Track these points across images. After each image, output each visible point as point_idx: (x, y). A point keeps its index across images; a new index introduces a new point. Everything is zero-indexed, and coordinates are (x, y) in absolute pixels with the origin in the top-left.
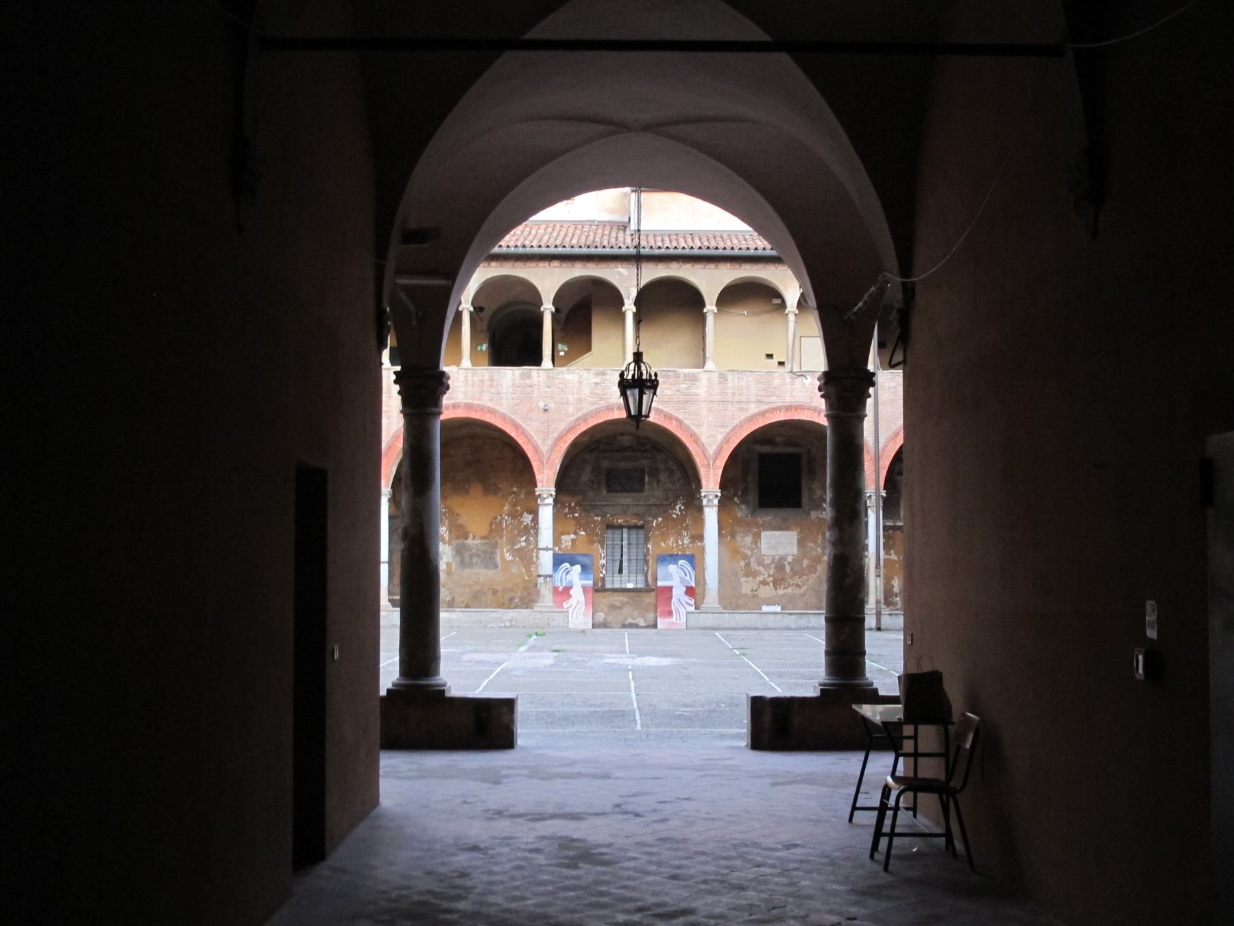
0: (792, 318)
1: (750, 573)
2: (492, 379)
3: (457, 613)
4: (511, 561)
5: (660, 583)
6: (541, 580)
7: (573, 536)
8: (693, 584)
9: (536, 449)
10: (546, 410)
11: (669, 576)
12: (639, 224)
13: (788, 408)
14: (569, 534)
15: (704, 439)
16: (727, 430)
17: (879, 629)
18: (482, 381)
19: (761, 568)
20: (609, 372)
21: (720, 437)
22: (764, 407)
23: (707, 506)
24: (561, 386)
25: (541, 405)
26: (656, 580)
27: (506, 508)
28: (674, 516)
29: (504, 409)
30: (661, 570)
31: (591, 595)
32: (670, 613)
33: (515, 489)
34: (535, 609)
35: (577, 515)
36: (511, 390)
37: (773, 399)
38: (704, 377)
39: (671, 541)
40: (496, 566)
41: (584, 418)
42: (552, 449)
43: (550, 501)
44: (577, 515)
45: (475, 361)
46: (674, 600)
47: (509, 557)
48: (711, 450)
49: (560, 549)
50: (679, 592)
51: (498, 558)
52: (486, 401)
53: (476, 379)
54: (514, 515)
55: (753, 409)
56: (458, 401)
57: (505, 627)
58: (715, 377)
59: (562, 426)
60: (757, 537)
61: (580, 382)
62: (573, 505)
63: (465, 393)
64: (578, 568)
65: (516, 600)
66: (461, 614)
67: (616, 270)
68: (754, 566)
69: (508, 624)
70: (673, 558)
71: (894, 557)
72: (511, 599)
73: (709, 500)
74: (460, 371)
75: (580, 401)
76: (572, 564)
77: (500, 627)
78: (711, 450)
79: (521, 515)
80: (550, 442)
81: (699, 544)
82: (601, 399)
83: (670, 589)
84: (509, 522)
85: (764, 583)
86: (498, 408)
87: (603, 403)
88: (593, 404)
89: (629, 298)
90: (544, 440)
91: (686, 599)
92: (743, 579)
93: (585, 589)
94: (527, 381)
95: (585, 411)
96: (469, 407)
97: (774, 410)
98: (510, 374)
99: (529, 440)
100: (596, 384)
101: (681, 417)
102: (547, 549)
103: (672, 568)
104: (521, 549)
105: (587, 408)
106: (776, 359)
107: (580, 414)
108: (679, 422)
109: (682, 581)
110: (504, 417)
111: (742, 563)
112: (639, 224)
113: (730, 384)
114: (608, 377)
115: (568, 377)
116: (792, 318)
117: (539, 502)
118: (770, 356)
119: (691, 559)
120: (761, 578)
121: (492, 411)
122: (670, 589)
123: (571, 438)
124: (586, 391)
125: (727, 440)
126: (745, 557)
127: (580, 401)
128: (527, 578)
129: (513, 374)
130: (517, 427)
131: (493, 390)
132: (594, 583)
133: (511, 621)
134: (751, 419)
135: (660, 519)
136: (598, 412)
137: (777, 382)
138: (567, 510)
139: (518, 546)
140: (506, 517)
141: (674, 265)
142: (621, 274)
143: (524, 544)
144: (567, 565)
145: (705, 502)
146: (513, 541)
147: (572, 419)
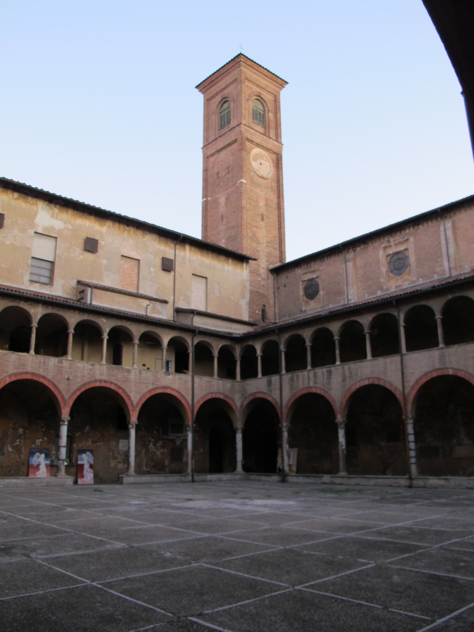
0: (165, 350)
1: (114, 458)
2: (44, 362)
3: (20, 480)
4: (12, 452)
5: (79, 462)
6: (61, 462)
7: (41, 440)
8: (92, 463)
9: (63, 397)
10: (68, 379)
11: (82, 459)
12: (91, 301)
13: (164, 387)
14: (39, 439)
15: (133, 398)
16: (141, 395)
17: (193, 481)
18: (40, 362)
19: (119, 456)
20: (96, 365)
21: (138, 398)
22: (155, 386)
23: (132, 428)
24: (75, 368)
25: (66, 376)
26: (77, 460)
27: (11, 425)
28: (85, 432)
29: (50, 377)
30: (79, 457)
31: (49, 468)
32: (83, 477)
33: (16, 416)
34: (59, 476)
35: (44, 430)
36: (53, 368)
37: (158, 383)
38: (133, 371)
39: (83, 443)
40: (4, 454)
41: (84, 385)
42: (70, 398)
43: (66, 423)
44: (44, 430)
45: (37, 352)
46: (85, 470)
47: (10, 449)
48: (135, 403)
49: (35, 446)
50: (86, 467)
51: (5, 450)
52: (41, 372)
53: (37, 361)
54: (15, 429)
55: (151, 387)
56: (28, 371)
57: (44, 486)
58: (138, 373)
59: (74, 387)
60: (118, 442)
61: (84, 368)
62: (42, 425)
63: (32, 367)
64: (43, 456)
65: (13, 471)
66: (22, 480)
67: (101, 319)
68: (116, 455)
69: (45, 484)
70: (82, 451)
71: (166, 451)
72: (10, 471)
73: (133, 426)
74: (30, 356)
75: (83, 376)
76: (41, 453)
77: (41, 486)
78: (135, 403)
79: (18, 429)
80: (69, 395)
81: (95, 445)
82: (92, 377)
83: (82, 466)
84: (12, 432)
85: (119, 462)
86: (47, 376)
87: (93, 379)
88: (89, 378)
89: (105, 332)
90: (66, 393)
91: (90, 470)
92: (112, 461)
93: (47, 465)
94: (61, 365)
95: (85, 381)
96: (33, 374)
97: (158, 388)
98: (53, 361)
99: (60, 392)
100: (91, 369)
101: (124, 388)
102: (64, 447)
103: (84, 456)
104: (17, 445)
105: (86, 380)
106: (147, 366)
107: (83, 382)
108: (123, 390)
109: (88, 461)
110: (49, 381)
111: (111, 454)
112: (91, 301)
113: (143, 375)
114: (95, 367)
115: (79, 365)
116: (165, 350)
117: (61, 423)
118: (144, 365)
119: (91, 451)
120: (118, 460)
121: (44, 377)
122: (82, 466)
123: (78, 393)
124: (86, 372)
125: (140, 399)
126: (113, 451)
127: (83, 376)
128: (18, 460)
129: (55, 361)
130: (55, 386)
131: (45, 367)
132: (51, 463)
133: (47, 483)
134: (150, 391)
135: (79, 433)
136: (89, 383)
137: (159, 376)
138: (39, 427)
139: (15, 444)
140: (11, 430)
141: (124, 321)
142: (103, 322)
143: (18, 443)
144: (38, 454)
145: (130, 426)
146: (13, 441)
147: (79, 385)
